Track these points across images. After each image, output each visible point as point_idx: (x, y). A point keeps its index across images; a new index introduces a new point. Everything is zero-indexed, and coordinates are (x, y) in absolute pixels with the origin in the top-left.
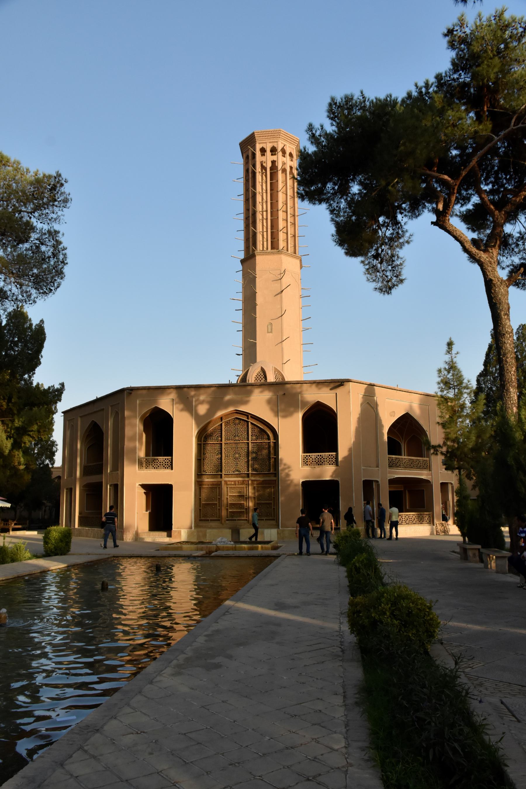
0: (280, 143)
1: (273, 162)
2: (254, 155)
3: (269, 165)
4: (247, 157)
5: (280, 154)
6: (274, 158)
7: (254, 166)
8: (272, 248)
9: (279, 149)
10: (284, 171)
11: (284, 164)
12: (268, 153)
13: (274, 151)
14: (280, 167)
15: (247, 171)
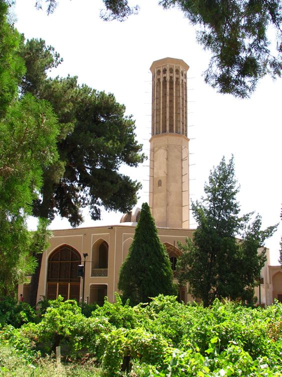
0: (181, 67)
1: (177, 79)
2: (165, 71)
3: (175, 80)
4: (159, 72)
5: (181, 74)
6: (178, 76)
7: (165, 78)
8: (176, 132)
9: (181, 71)
10: (182, 85)
11: (182, 81)
12: (175, 72)
13: (177, 71)
14: (181, 82)
15: (159, 80)
